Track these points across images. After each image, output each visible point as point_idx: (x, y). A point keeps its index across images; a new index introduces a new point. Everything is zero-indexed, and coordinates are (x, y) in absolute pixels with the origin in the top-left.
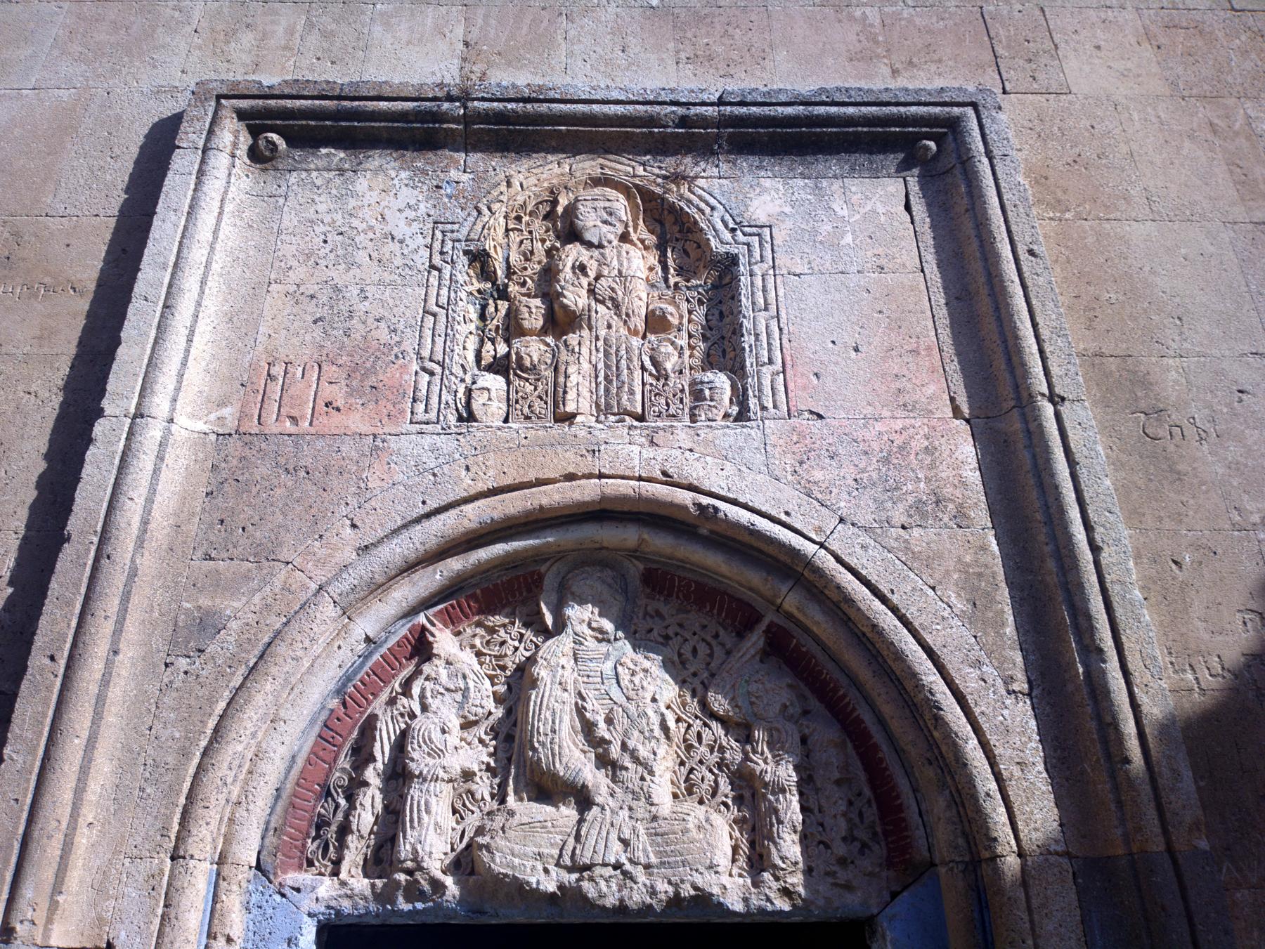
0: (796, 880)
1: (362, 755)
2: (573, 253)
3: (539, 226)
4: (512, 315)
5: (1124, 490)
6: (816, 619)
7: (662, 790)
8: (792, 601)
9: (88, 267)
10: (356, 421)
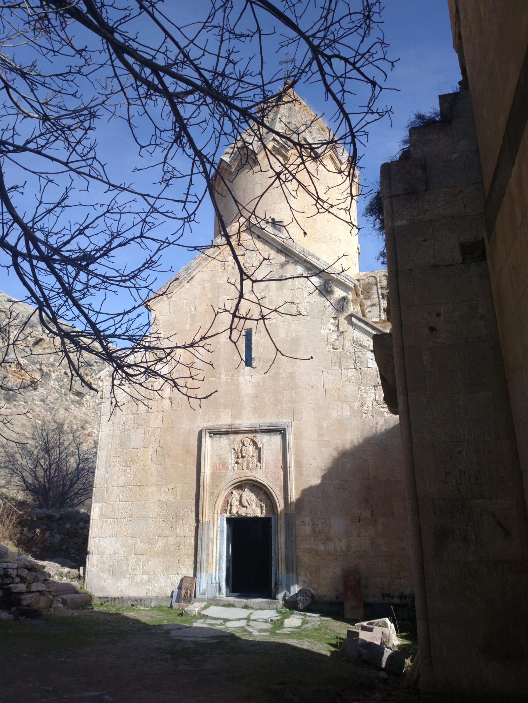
1: (228, 503)
2: (244, 448)
5: (295, 478)
7: (254, 507)
9: (195, 453)
10: (223, 471)
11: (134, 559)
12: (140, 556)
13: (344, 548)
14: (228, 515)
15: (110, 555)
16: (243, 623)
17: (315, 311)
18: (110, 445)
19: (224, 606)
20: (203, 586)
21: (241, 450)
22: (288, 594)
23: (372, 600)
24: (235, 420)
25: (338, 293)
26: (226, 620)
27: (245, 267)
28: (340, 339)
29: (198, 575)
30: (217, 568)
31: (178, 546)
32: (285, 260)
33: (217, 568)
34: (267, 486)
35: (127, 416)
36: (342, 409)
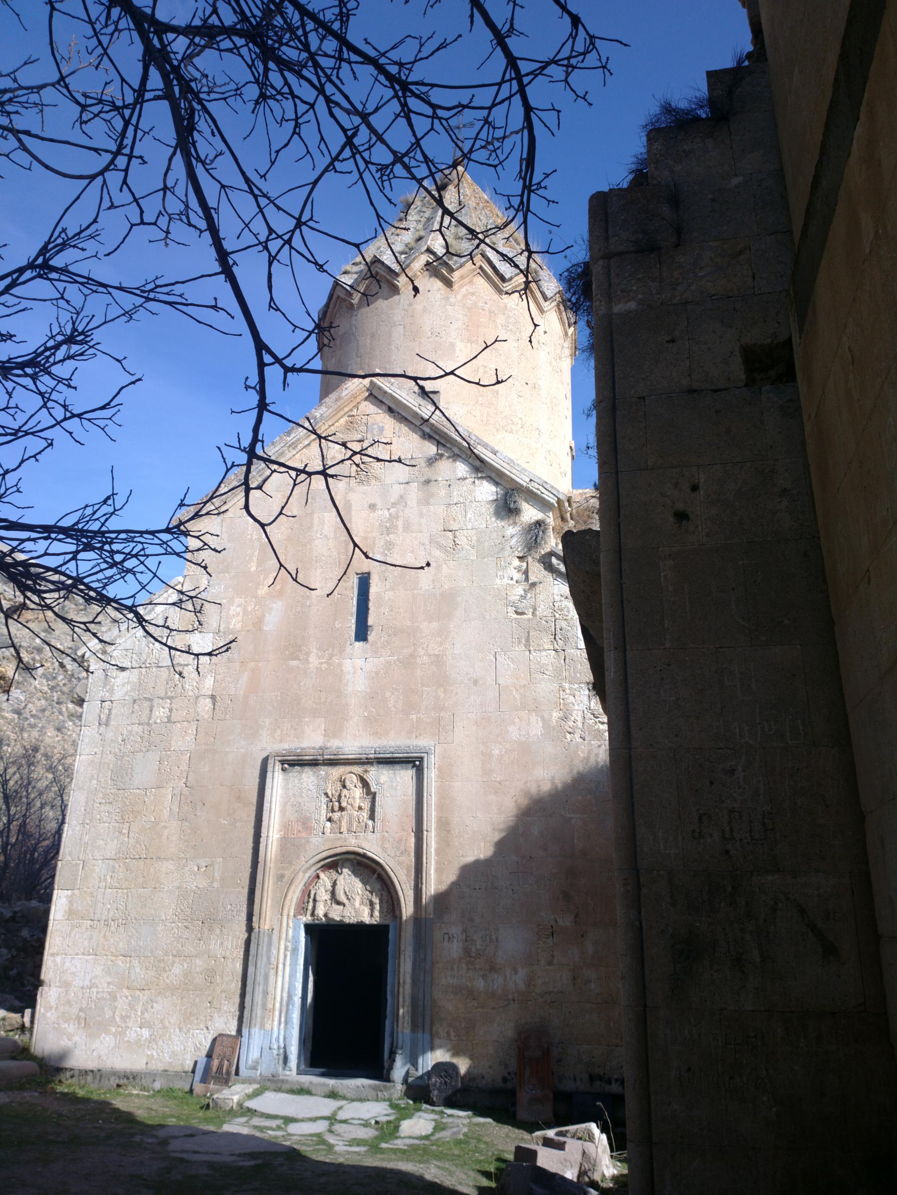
0: (378, 919)
2: (345, 792)
3: (339, 783)
4: (332, 807)
6: (383, 873)
7: (357, 904)
8: (380, 870)
9: (254, 799)
10: (304, 835)
11: (126, 997)
12: (138, 992)
13: (522, 986)
14: (308, 919)
15: (82, 988)
16: (321, 1127)
17: (486, 544)
18: (95, 782)
19: (292, 1092)
20: (254, 1054)
21: (340, 796)
22: (413, 1071)
23: (569, 1086)
24: (332, 741)
25: (530, 513)
26: (289, 1120)
27: (363, 463)
28: (529, 595)
29: (245, 1031)
30: (283, 1019)
31: (210, 975)
32: (435, 452)
33: (283, 1019)
34: (384, 864)
35: (129, 728)
36: (529, 724)
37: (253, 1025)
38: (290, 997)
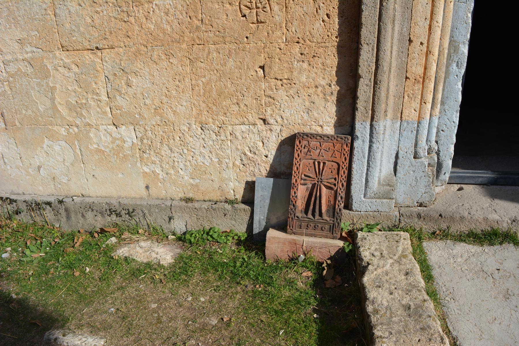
12: (88, 56)
29: (362, 128)
30: (439, 96)
37: (379, 114)
38: (453, 45)
